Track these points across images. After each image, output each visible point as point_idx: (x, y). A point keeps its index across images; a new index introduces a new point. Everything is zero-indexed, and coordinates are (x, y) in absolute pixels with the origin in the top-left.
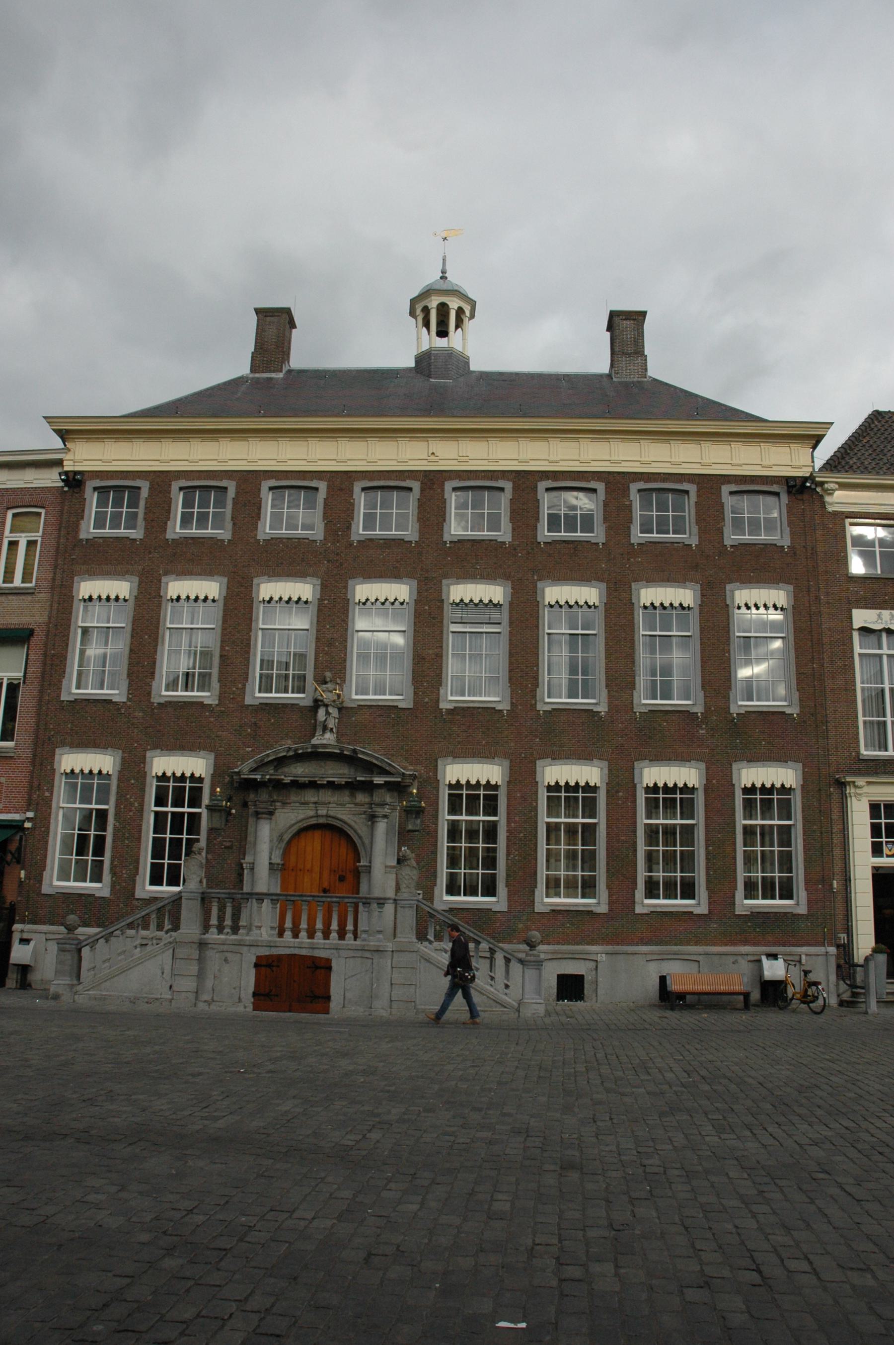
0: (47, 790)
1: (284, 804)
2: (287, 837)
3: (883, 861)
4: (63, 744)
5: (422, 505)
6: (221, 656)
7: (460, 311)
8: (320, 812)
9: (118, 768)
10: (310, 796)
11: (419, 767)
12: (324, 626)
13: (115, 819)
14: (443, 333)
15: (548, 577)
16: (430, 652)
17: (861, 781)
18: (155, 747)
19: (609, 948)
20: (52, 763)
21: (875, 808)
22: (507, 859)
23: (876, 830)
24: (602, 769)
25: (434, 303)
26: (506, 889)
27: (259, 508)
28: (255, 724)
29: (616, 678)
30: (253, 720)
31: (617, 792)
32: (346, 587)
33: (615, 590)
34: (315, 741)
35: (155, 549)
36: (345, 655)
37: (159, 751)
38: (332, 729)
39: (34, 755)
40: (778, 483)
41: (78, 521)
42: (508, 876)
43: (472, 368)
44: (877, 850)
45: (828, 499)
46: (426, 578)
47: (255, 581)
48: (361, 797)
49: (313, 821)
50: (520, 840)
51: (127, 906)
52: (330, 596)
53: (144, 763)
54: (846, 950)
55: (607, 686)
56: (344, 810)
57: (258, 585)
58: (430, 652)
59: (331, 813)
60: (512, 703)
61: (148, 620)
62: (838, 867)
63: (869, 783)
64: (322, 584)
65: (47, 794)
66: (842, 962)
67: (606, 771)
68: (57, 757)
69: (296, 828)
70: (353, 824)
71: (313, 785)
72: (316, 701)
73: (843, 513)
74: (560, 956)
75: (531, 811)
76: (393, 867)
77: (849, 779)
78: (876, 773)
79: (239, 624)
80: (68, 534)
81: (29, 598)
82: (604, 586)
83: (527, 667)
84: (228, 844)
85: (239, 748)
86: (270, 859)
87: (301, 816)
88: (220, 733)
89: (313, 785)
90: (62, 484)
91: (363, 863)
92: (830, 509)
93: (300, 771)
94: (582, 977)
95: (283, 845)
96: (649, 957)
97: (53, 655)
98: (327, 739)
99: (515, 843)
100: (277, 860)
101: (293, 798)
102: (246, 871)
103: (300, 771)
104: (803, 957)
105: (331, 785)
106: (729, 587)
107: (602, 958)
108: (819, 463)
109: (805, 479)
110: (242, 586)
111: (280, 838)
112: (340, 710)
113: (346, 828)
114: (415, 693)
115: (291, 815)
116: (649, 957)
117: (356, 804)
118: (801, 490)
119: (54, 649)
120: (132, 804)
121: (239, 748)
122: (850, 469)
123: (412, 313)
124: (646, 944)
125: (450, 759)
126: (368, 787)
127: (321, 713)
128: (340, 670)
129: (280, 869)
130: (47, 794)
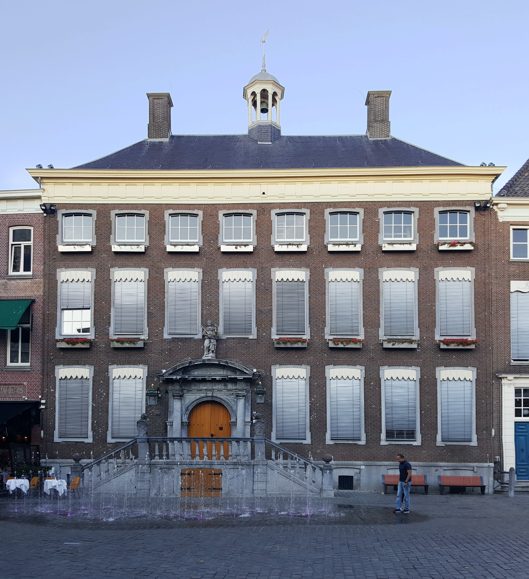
0: (52, 388)
1: (188, 391)
2: (190, 408)
3: (522, 419)
4: (59, 364)
5: (258, 224)
6: (148, 313)
7: (275, 94)
8: (208, 395)
9: (92, 375)
10: (203, 387)
11: (261, 370)
12: (206, 295)
13: (93, 402)
14: (264, 111)
15: (331, 266)
16: (266, 308)
17: (511, 377)
18: (113, 363)
19: (367, 463)
20: (54, 374)
21: (518, 392)
22: (310, 417)
23: (518, 403)
24: (361, 370)
25: (258, 89)
26: (310, 433)
27: (165, 227)
28: (170, 349)
29: (369, 321)
30: (169, 347)
31: (370, 382)
32: (217, 273)
33: (369, 272)
34: (204, 358)
35: (104, 252)
36: (219, 310)
37: (116, 365)
38: (213, 351)
39: (43, 370)
40: (469, 205)
41: (55, 235)
42: (311, 426)
43: (282, 134)
44: (518, 413)
45: (500, 214)
46: (262, 268)
47: (165, 270)
48: (230, 386)
49: (205, 399)
50: (317, 407)
51: (104, 447)
52: (208, 279)
53: (108, 372)
54: (499, 465)
55: (364, 326)
56: (222, 393)
57: (167, 272)
58: (266, 308)
59: (214, 395)
60: (311, 336)
61: (104, 293)
62: (495, 422)
63: (515, 378)
64: (203, 272)
65: (52, 390)
66: (497, 471)
67: (364, 371)
68: (56, 370)
69: (195, 403)
70: (226, 400)
71: (204, 381)
72: (203, 336)
73: (509, 222)
74: (340, 466)
75: (323, 392)
76: (249, 422)
77: (503, 376)
78: (520, 372)
79: (158, 295)
80: (50, 243)
81: (30, 281)
82: (362, 270)
83: (319, 316)
84: (159, 413)
85: (162, 362)
86: (182, 420)
87: (198, 397)
88: (150, 355)
89: (204, 381)
90: (42, 212)
91: (233, 420)
92: (501, 220)
93: (197, 373)
94: (352, 477)
95: (188, 412)
96: (389, 467)
97: (49, 314)
98: (209, 356)
99: (314, 409)
100: (185, 420)
101: (193, 388)
102: (168, 427)
103: (197, 373)
104: (475, 468)
105: (214, 381)
106: (436, 269)
107: (363, 467)
108: (496, 192)
109: (487, 202)
110: (158, 273)
111: (187, 409)
112: (217, 341)
113: (223, 402)
114: (258, 330)
115: (191, 397)
116: (389, 467)
117: (228, 390)
118: (483, 208)
119: (48, 311)
120: (102, 394)
121: (162, 362)
122: (516, 194)
123: (245, 95)
124: (387, 461)
125: (278, 366)
126: (234, 381)
127: (207, 342)
128: (216, 319)
129: (187, 425)
130: (52, 390)
